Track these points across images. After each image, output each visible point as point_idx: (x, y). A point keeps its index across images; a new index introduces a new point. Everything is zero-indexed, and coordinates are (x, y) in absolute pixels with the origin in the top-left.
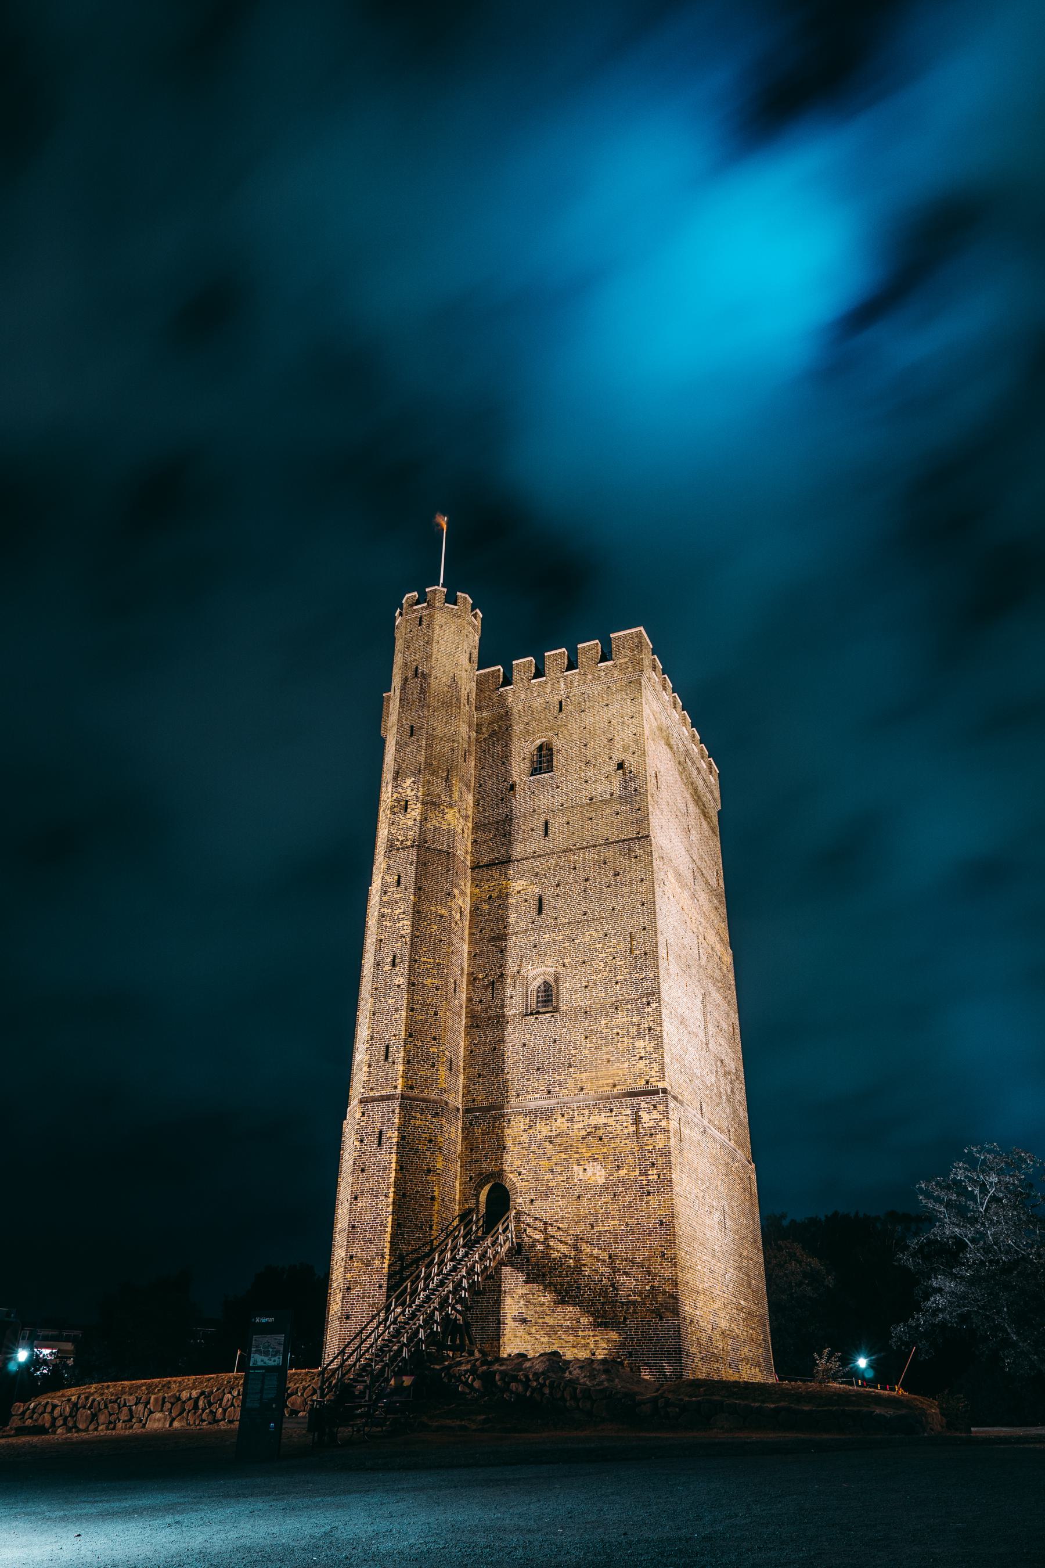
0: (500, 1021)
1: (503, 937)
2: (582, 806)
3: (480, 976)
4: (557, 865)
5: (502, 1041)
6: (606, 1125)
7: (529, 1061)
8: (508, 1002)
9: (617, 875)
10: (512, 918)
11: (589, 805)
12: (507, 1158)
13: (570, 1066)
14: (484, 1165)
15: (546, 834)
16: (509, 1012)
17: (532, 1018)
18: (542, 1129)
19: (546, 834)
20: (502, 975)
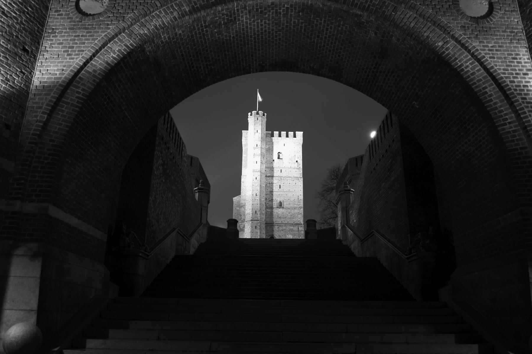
0: (272, 208)
1: (272, 192)
2: (289, 168)
3: (268, 199)
4: (284, 179)
5: (273, 212)
6: (293, 229)
7: (278, 216)
8: (274, 204)
9: (296, 184)
10: (274, 188)
11: (290, 168)
12: (274, 232)
13: (286, 218)
14: (270, 233)
15: (281, 172)
16: (274, 206)
17: (278, 209)
18: (281, 228)
19: (281, 172)
20: (272, 199)
